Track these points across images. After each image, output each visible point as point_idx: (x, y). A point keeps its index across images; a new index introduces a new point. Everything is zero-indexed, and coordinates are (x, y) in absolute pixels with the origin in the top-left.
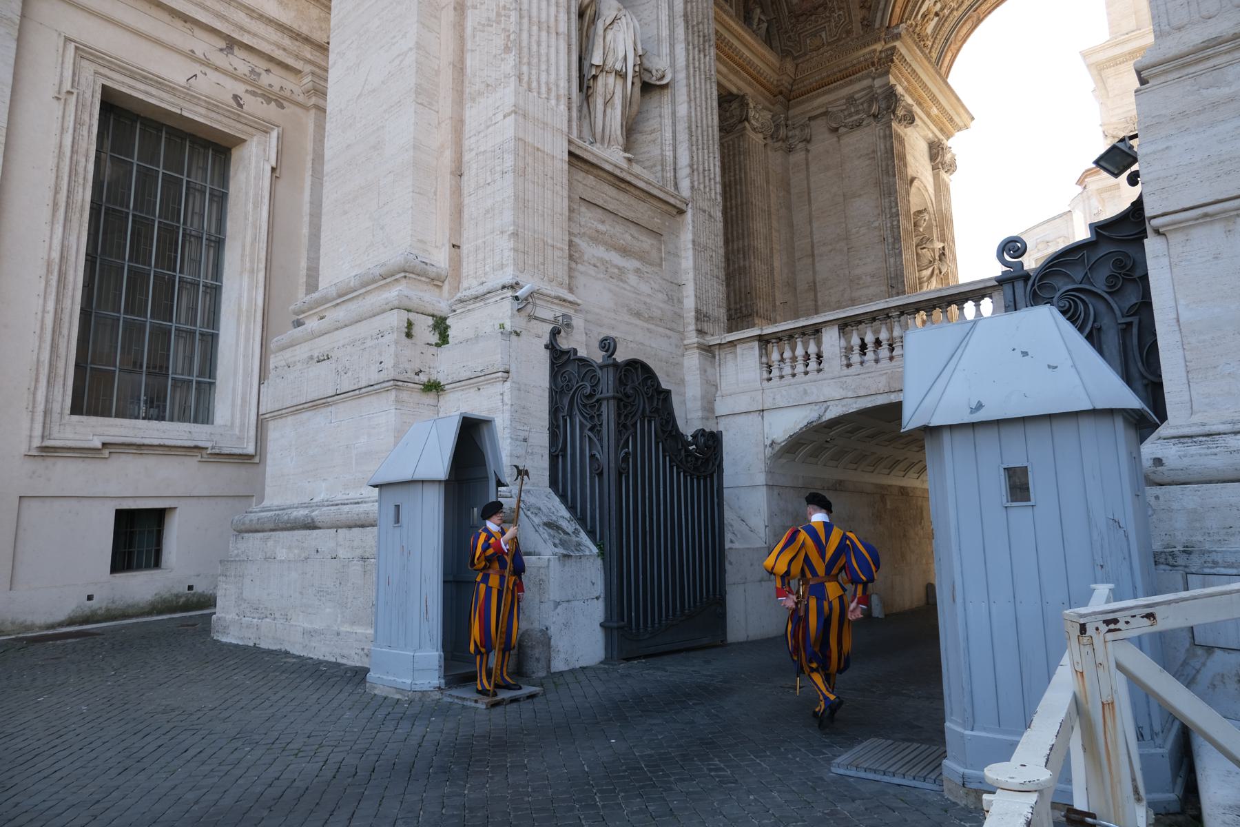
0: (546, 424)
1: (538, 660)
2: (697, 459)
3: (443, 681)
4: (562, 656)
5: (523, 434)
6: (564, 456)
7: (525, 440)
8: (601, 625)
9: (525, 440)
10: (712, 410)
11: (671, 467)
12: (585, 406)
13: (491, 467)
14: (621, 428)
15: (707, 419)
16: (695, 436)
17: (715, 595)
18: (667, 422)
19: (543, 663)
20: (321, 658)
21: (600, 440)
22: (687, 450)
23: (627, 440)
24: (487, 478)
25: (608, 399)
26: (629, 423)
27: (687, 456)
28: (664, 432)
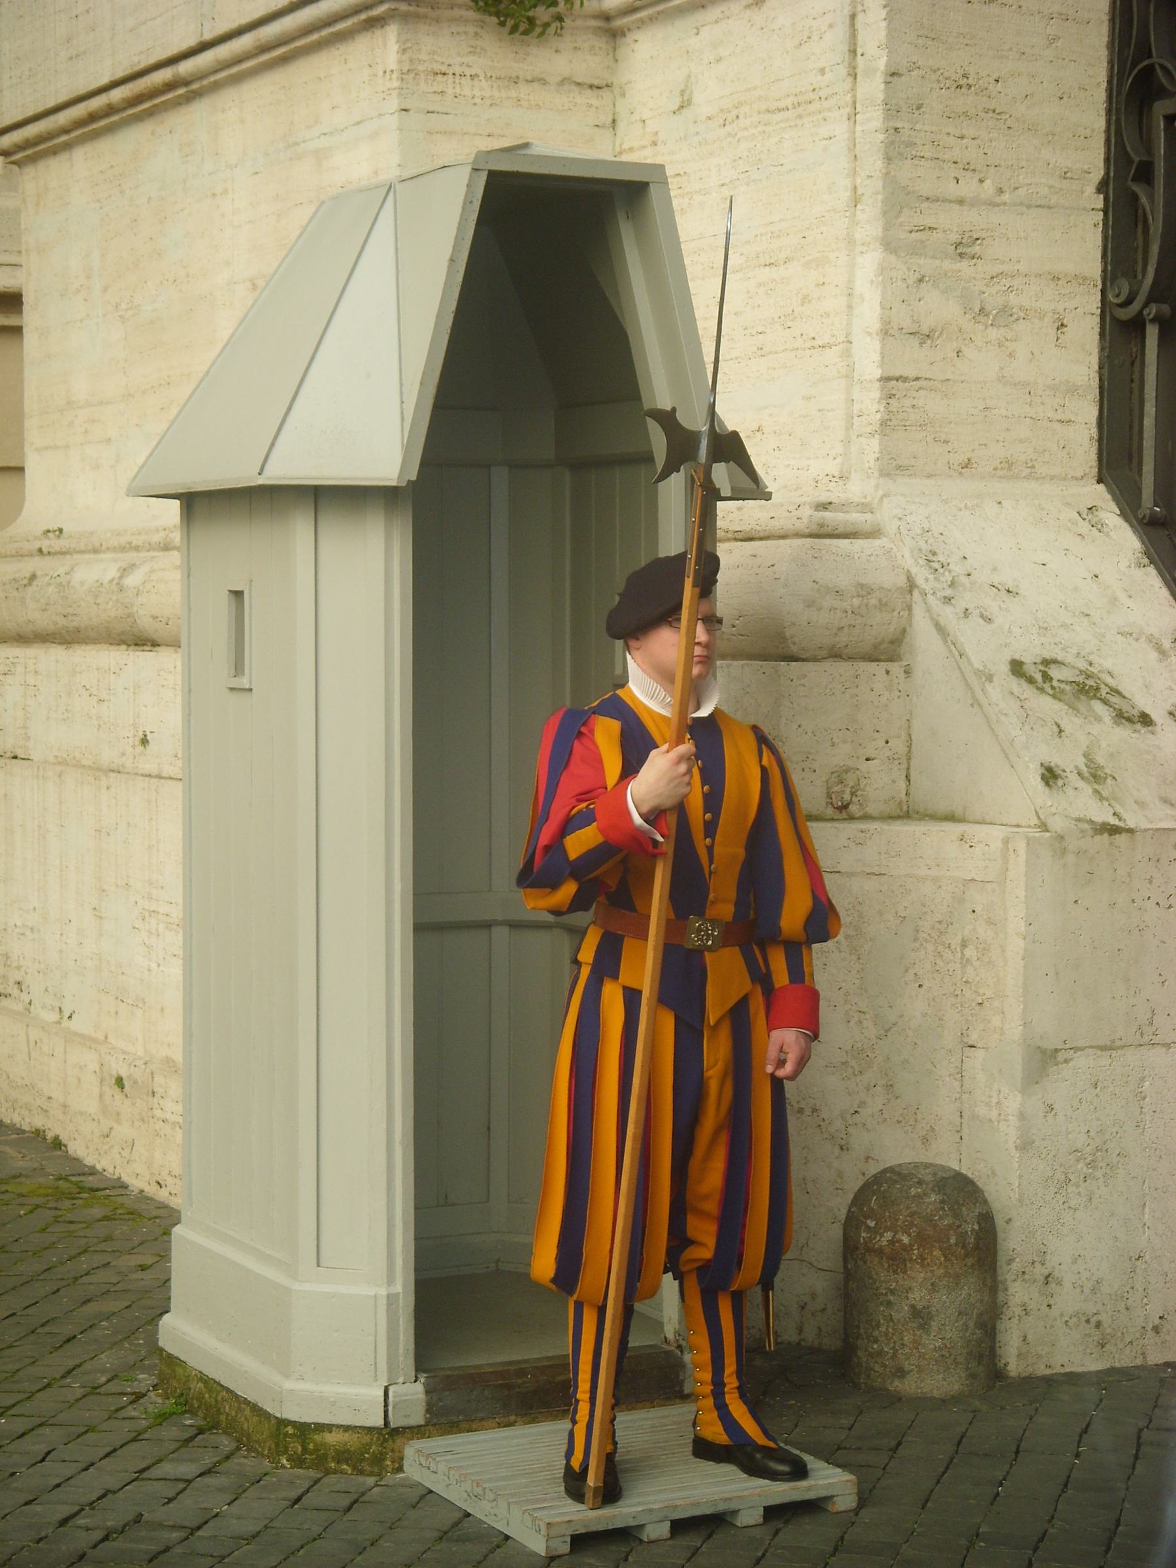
0: (1092, 160)
1: (921, 1316)
3: (412, 1395)
4: (1068, 1301)
5: (952, 222)
7: (964, 249)
9: (964, 249)
19: (948, 1328)
20: (151, 1190)
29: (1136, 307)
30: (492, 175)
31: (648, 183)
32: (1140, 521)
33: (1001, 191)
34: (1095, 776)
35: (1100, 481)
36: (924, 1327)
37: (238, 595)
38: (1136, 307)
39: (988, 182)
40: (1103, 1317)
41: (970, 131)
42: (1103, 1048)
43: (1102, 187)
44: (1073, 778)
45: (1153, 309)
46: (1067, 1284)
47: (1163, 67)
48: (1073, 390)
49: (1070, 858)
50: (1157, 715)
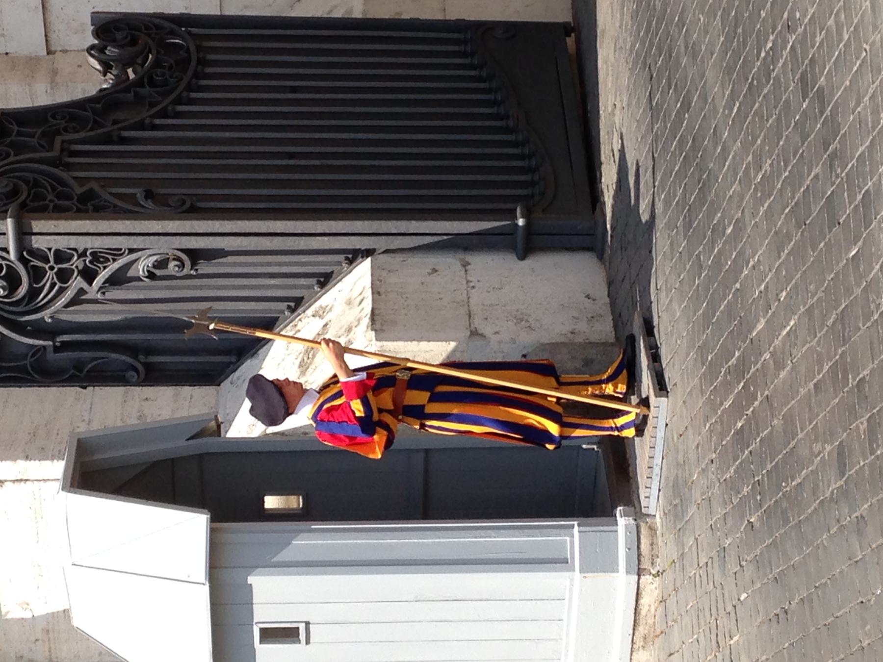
0: (71, 393)
2: (157, 64)
4: (582, 326)
6: (150, 350)
8: (522, 257)
10: (32, 62)
11: (178, 115)
12: (33, 293)
13: (179, 446)
14: (89, 205)
15: (54, 72)
16: (107, 67)
17: (465, 42)
18: (73, 118)
21: (116, 253)
22: (139, 83)
23: (115, 195)
24: (201, 458)
25: (23, 234)
26: (79, 190)
27: (152, 83)
28: (97, 125)
29: (140, 367)
30: (72, 485)
31: (79, 440)
32: (238, 361)
33: (84, 421)
34: (349, 330)
35: (219, 385)
36: (592, 361)
37: (262, 630)
38: (140, 367)
39: (79, 425)
40: (589, 316)
41: (55, 432)
42: (470, 317)
43: (85, 388)
44: (350, 337)
45: (142, 358)
46: (575, 327)
47: (32, 357)
48: (176, 395)
49: (384, 328)
50: (323, 322)
